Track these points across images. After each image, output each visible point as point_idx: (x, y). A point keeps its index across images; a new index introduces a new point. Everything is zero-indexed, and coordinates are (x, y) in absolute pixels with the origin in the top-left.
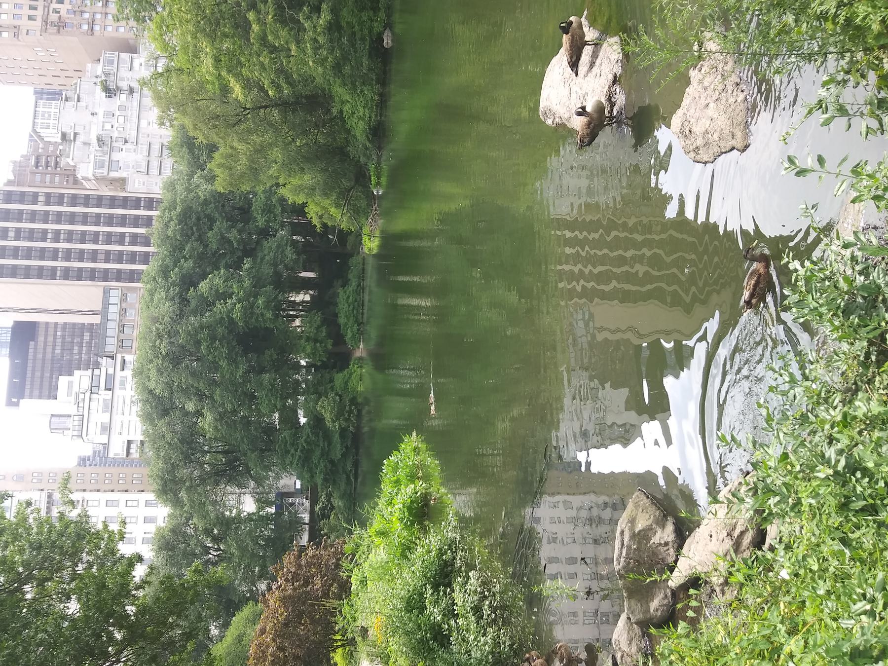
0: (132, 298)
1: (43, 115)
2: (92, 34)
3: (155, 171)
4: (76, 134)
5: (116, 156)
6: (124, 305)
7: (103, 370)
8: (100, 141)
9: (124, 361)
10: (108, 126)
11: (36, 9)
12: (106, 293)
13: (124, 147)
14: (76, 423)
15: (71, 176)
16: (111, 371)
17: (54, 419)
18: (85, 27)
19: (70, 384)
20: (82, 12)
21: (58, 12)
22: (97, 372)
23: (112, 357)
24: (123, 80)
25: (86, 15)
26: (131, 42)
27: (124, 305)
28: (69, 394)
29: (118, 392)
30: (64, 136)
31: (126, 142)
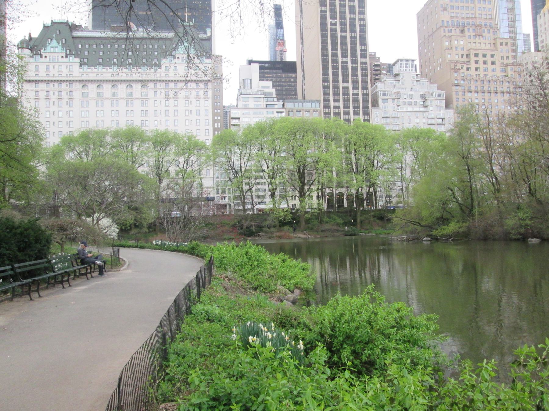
0: (316, 114)
1: (407, 64)
2: (453, 86)
3: (384, 121)
4: (399, 80)
5: (390, 101)
6: (311, 111)
7: (277, 103)
8: (398, 93)
9: (281, 113)
10: (405, 96)
11: (462, 57)
12: (318, 101)
13: (395, 105)
14: (248, 91)
15: (376, 79)
16: (276, 106)
17: (249, 81)
18: (456, 82)
19: (268, 87)
20: (464, 80)
21: (462, 68)
22: (275, 100)
23: (283, 106)
24: (431, 102)
25: (462, 82)
26: (451, 105)
27: (311, 111)
28: (263, 87)
29: (265, 111)
30: (397, 75)
31: (398, 106)
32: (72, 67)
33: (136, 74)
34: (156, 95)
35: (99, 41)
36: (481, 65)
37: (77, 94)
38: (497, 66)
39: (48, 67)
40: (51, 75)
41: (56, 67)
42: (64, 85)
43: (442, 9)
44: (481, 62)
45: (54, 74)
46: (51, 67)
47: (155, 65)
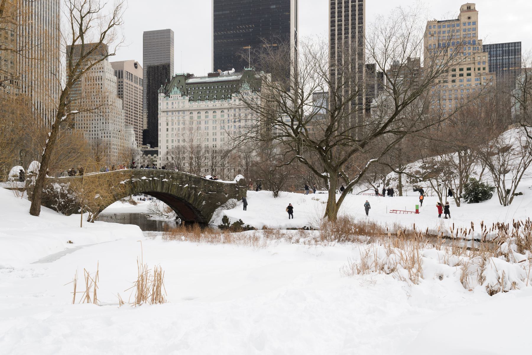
32: (184, 103)
33: (218, 104)
34: (229, 116)
35: (199, 85)
36: (457, 78)
37: (187, 118)
38: (473, 77)
39: (173, 103)
40: (174, 107)
41: (177, 103)
42: (181, 113)
43: (430, 36)
44: (458, 76)
45: (175, 105)
46: (174, 103)
47: (229, 98)
